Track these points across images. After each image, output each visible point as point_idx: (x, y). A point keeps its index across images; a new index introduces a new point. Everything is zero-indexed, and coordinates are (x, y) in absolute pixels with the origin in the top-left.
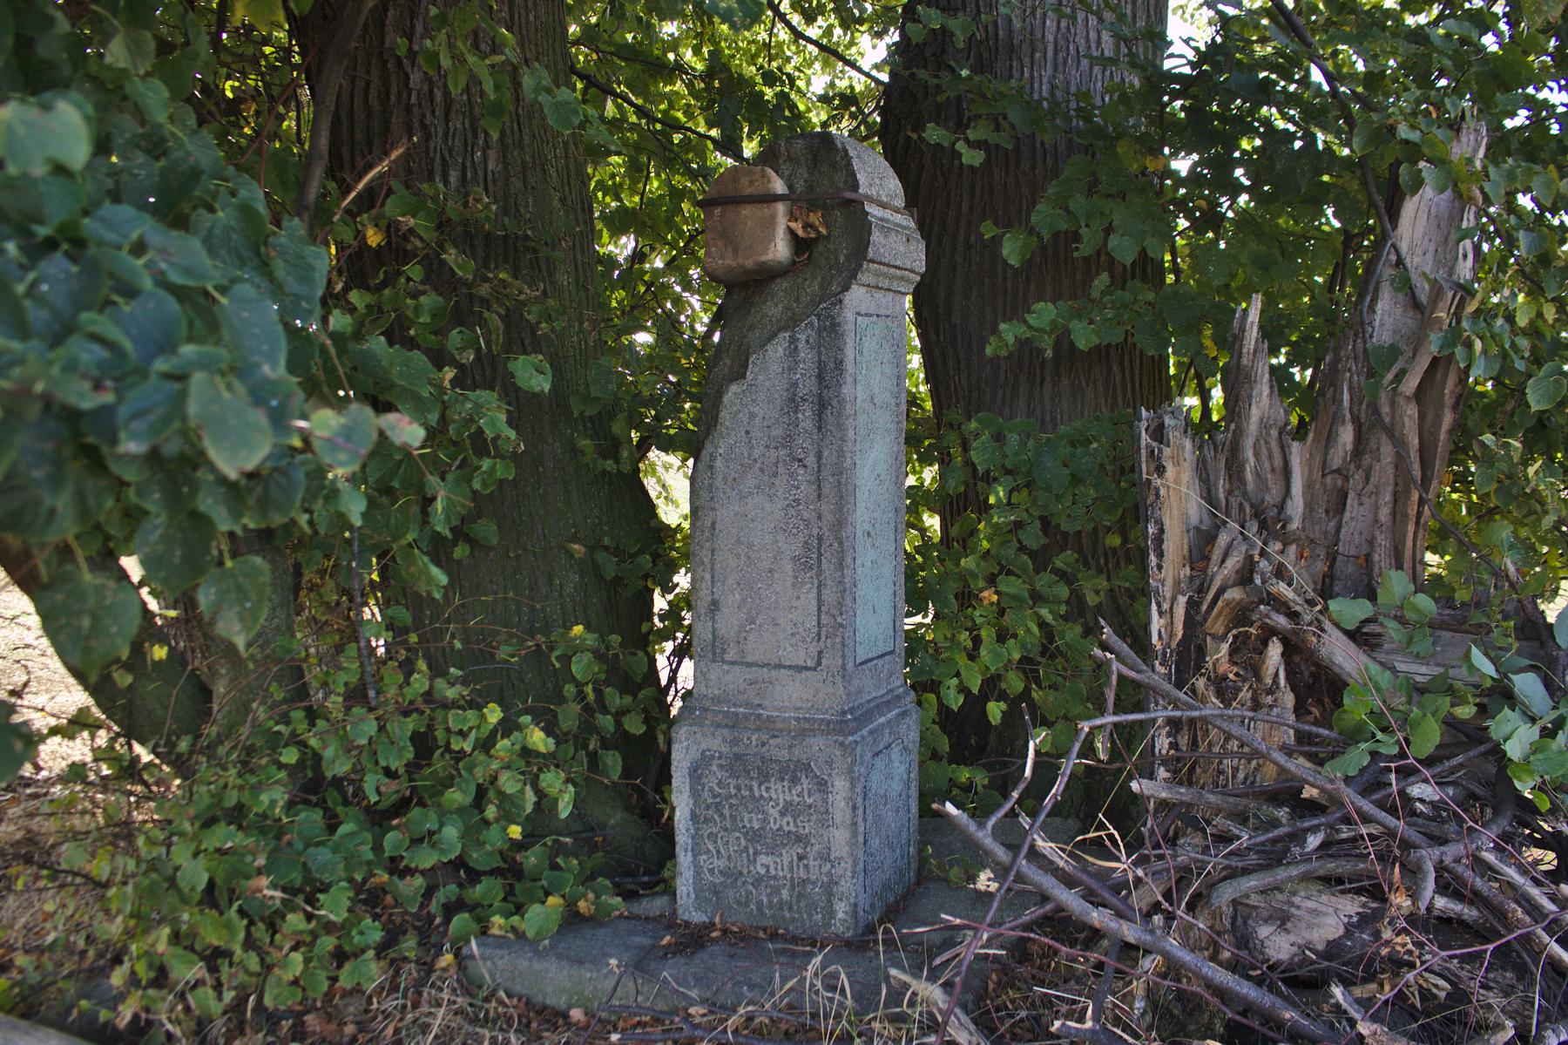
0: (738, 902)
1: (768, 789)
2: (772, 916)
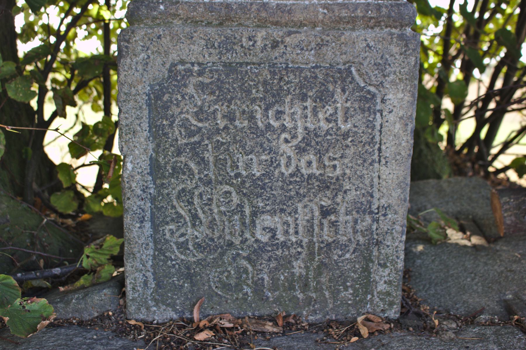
0: (225, 286)
1: (279, 114)
2: (277, 300)
